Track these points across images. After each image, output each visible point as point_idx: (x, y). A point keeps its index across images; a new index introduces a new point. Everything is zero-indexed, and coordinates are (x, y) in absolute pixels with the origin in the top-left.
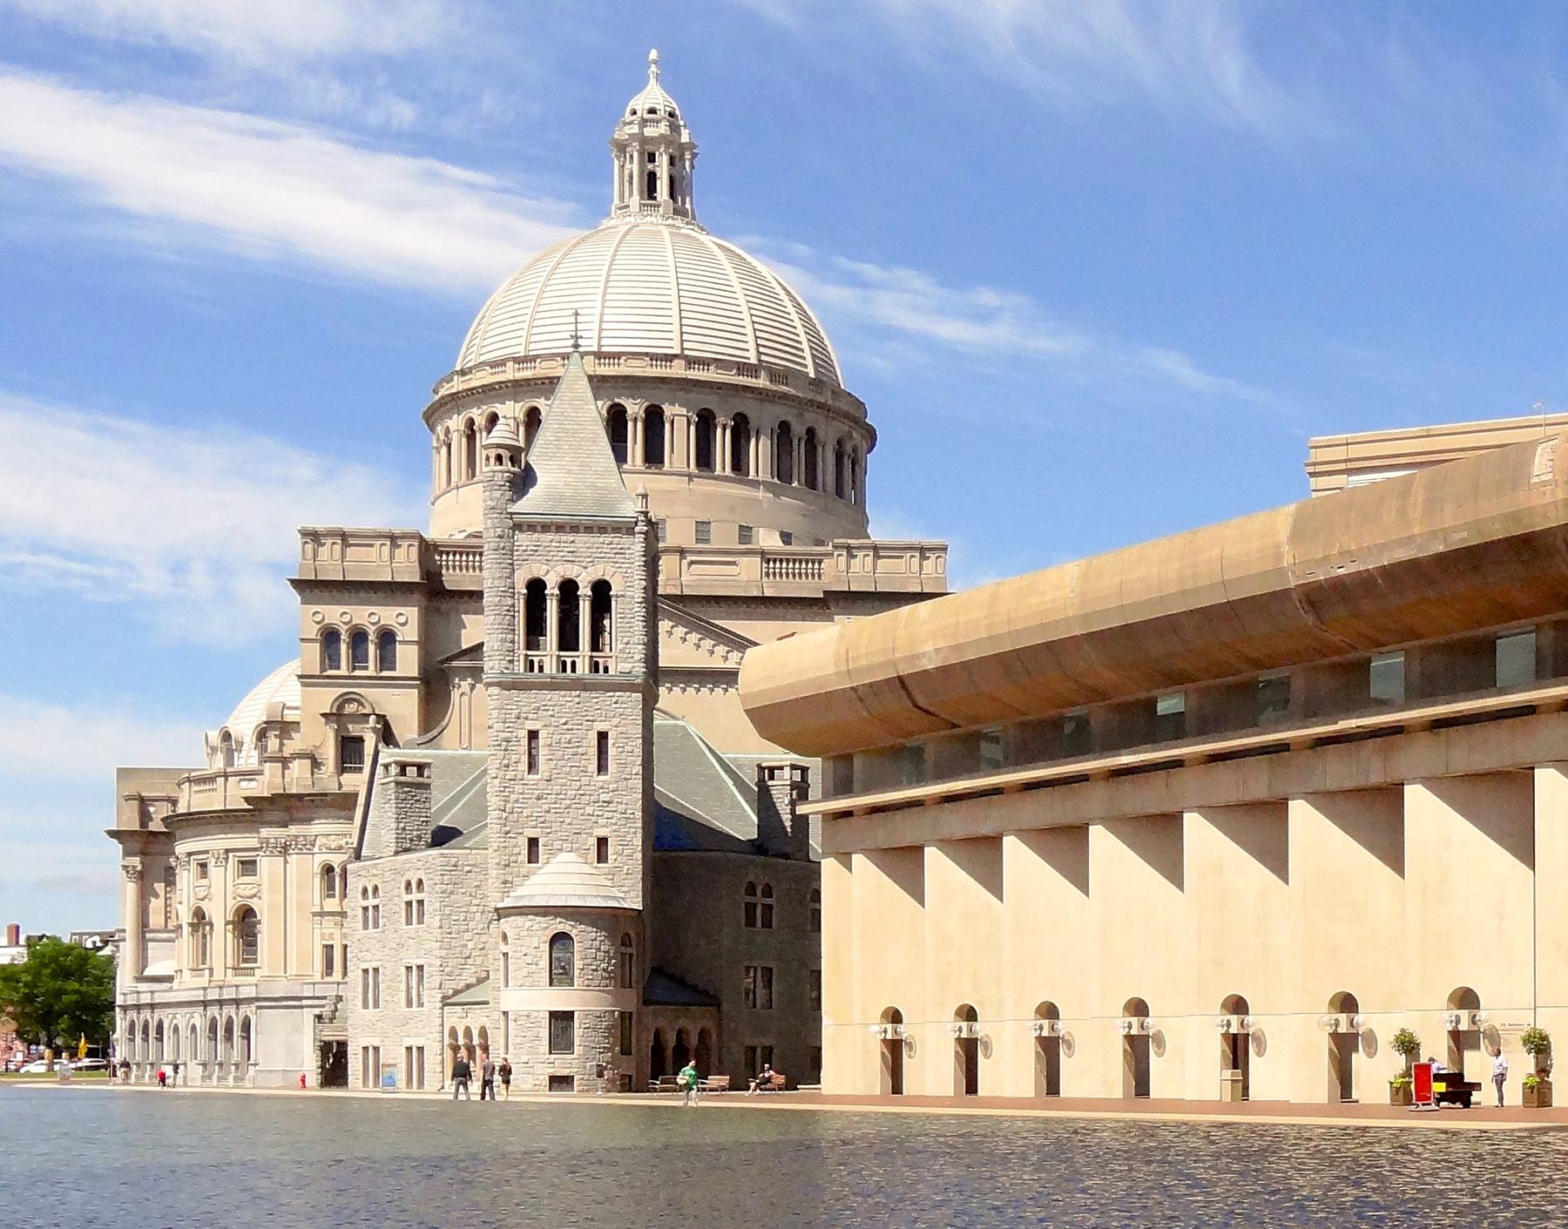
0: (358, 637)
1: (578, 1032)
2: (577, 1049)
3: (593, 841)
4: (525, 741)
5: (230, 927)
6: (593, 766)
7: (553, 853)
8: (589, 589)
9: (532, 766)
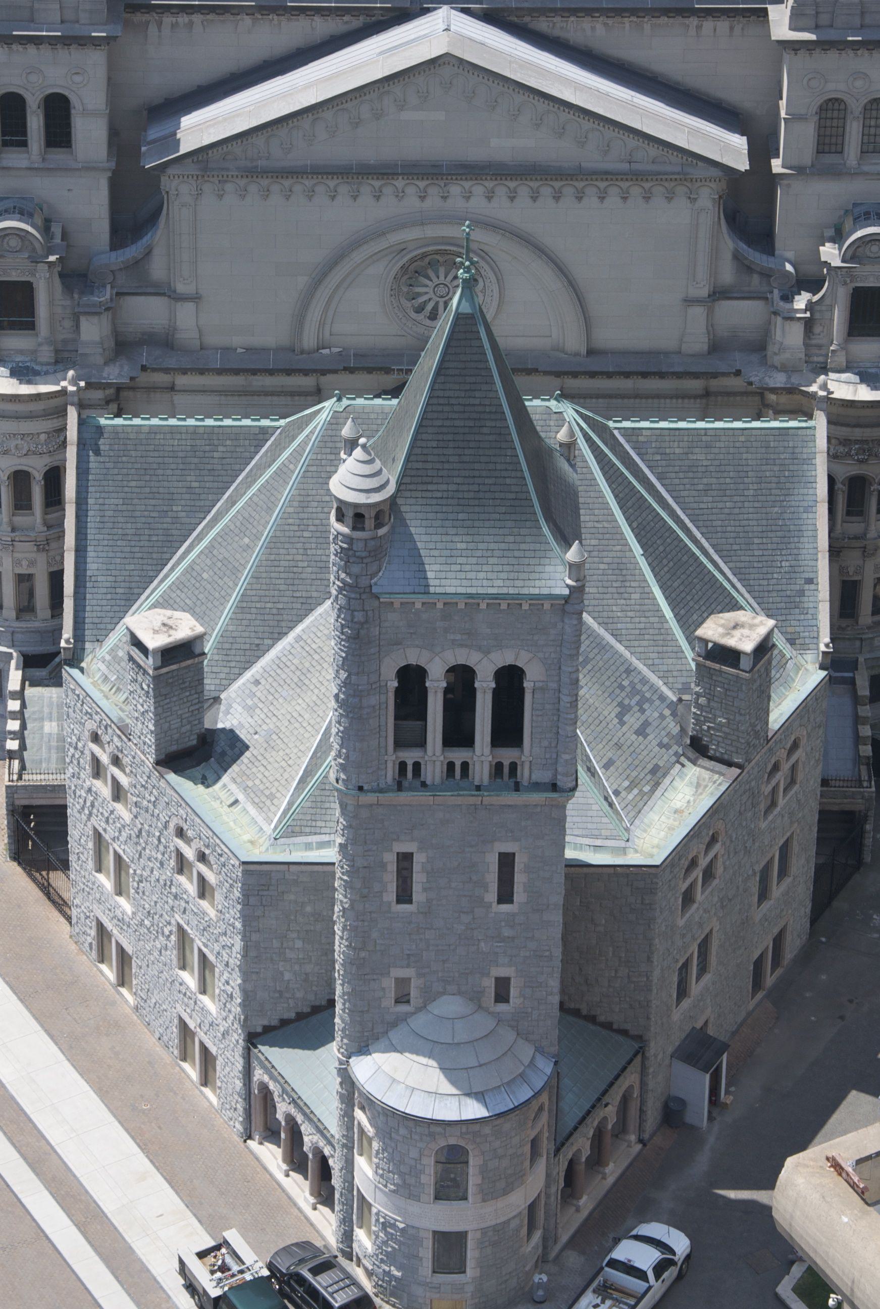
1: (472, 1254)
2: (471, 1270)
3: (489, 984)
4: (393, 867)
6: (492, 895)
7: (429, 997)
8: (491, 677)
9: (404, 896)
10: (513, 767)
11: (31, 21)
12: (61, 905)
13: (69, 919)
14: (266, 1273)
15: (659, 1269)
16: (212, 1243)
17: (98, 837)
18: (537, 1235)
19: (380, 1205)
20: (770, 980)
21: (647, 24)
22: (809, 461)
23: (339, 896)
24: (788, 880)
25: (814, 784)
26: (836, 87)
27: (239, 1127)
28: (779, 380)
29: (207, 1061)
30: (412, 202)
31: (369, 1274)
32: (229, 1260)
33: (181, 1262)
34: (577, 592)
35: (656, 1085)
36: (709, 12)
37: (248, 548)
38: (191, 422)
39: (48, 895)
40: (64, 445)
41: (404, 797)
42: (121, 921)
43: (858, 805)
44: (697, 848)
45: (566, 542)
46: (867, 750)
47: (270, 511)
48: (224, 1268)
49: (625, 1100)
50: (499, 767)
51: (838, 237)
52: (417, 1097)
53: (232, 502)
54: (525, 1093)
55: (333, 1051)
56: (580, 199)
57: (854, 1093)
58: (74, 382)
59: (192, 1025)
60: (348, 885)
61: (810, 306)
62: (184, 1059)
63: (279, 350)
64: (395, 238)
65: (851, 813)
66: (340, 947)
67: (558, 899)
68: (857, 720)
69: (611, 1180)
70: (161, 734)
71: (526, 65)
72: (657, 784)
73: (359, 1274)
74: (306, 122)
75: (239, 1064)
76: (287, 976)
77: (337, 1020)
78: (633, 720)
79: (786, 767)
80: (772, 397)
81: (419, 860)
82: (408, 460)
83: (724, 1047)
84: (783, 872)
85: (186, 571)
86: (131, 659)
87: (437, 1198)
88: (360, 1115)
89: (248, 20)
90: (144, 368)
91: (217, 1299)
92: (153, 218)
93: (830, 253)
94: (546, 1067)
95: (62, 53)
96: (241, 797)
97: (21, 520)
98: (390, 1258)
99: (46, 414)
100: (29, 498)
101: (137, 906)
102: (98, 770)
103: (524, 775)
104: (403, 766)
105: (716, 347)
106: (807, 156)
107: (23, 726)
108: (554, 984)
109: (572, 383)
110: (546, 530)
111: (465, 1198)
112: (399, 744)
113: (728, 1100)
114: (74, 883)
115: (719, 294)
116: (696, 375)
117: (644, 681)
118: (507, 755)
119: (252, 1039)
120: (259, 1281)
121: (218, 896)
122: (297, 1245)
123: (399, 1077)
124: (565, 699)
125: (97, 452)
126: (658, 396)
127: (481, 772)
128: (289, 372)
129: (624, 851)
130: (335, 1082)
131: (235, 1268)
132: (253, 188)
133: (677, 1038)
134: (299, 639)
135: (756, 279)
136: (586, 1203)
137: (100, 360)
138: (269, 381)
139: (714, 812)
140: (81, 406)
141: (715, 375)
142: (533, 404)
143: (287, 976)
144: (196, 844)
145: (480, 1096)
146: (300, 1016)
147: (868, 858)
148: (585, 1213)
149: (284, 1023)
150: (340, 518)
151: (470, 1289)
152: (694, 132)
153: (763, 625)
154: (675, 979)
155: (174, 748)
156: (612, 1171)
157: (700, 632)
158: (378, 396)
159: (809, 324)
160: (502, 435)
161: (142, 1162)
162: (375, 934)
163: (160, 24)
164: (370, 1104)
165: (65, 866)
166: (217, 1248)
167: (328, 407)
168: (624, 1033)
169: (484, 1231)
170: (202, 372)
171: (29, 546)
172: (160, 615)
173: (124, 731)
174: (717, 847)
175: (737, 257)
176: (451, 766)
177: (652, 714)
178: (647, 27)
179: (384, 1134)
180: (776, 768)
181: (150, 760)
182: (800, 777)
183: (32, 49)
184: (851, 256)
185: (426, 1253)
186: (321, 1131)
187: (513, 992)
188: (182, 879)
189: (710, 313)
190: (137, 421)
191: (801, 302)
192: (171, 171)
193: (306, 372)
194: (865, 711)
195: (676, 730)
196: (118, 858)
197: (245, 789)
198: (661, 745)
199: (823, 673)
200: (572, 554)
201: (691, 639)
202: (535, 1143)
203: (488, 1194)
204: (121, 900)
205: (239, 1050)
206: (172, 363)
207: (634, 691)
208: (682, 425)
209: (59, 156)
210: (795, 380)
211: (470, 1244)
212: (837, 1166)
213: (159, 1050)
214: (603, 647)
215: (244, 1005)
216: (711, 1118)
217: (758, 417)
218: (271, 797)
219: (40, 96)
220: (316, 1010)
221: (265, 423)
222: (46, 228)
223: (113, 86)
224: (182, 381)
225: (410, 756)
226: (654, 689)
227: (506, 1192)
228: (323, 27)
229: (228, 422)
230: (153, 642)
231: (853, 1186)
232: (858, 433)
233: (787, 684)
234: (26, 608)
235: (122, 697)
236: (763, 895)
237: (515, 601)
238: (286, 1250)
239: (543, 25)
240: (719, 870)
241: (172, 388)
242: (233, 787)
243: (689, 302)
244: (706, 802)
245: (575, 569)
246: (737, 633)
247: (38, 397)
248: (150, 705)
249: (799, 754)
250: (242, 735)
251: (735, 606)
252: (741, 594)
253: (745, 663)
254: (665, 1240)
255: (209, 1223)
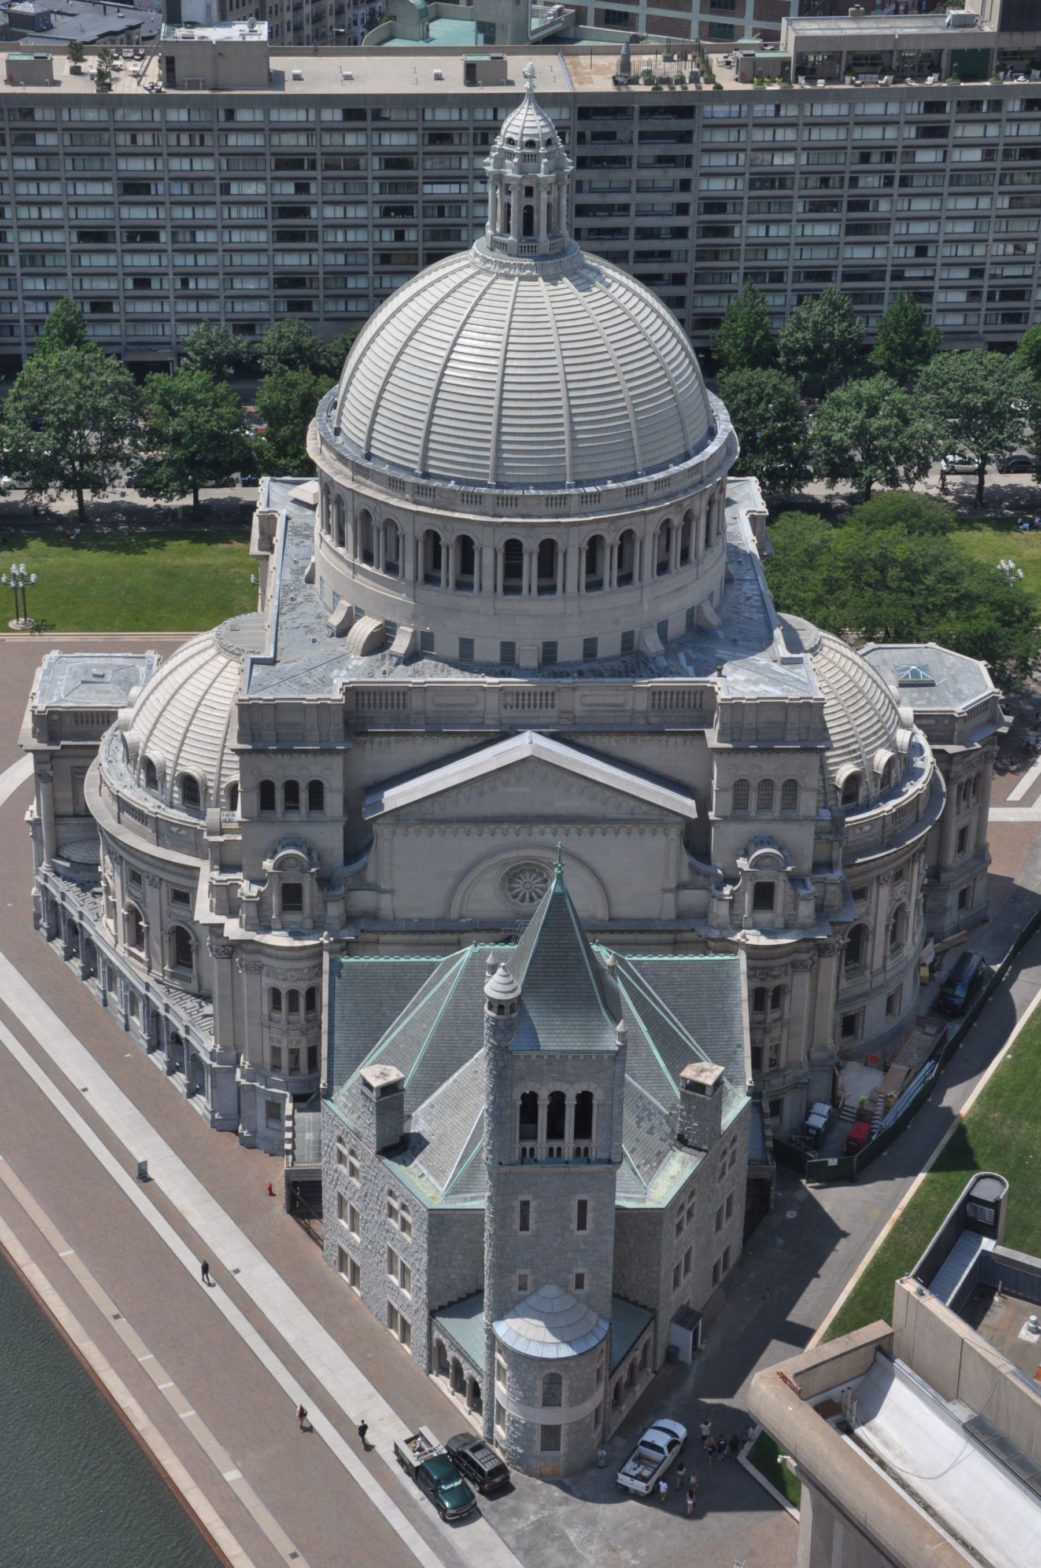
0: (291, 788)
1: (563, 1438)
2: (563, 1448)
3: (572, 1278)
4: (518, 1210)
5: (166, 938)
6: (574, 1225)
7: (538, 1285)
9: (524, 1226)
10: (586, 1150)
11: (303, 742)
12: (317, 1239)
13: (322, 1247)
14: (445, 1451)
15: (671, 1445)
16: (411, 1435)
17: (341, 1198)
18: (600, 1427)
19: (510, 1411)
20: (721, 1277)
21: (639, 740)
22: (737, 978)
23: (487, 1227)
24: (731, 1218)
25: (744, 1162)
26: (744, 773)
27: (424, 1366)
28: (716, 934)
29: (405, 1328)
30: (523, 837)
31: (504, 1452)
32: (423, 1445)
33: (396, 1446)
34: (623, 1048)
35: (662, 1338)
36: (672, 733)
37: (426, 1030)
38: (392, 960)
39: (309, 1234)
40: (319, 974)
41: (526, 1168)
42: (354, 1247)
43: (767, 1175)
44: (684, 1198)
45: (616, 1020)
46: (770, 1144)
47: (438, 1009)
48: (420, 1449)
49: (646, 1347)
50: (578, 1151)
51: (746, 854)
52: (532, 1345)
53: (416, 1004)
54: (594, 1342)
55: (482, 1318)
56: (604, 834)
57: (774, 1342)
58: (327, 938)
59: (396, 1306)
60: (493, 1220)
61: (732, 893)
62: (391, 1327)
63: (437, 920)
64: (503, 857)
65: (761, 1180)
66: (487, 1257)
67: (611, 1226)
68: (764, 1126)
69: (638, 1395)
70: (380, 1136)
71: (574, 762)
72: (660, 1162)
73: (498, 1452)
74: (453, 794)
75: (425, 1329)
76: (453, 1276)
77: (485, 1300)
78: (645, 1125)
79: (730, 1152)
80: (712, 944)
81: (533, 1205)
82: (527, 975)
83: (699, 1316)
84: (729, 1214)
85: (390, 1044)
86: (363, 1093)
87: (545, 1404)
88: (499, 1357)
89: (420, 739)
90: (363, 931)
91: (418, 1468)
92: (368, 847)
93: (743, 863)
94: (605, 1327)
95: (320, 759)
96: (425, 1172)
97: (292, 1018)
98: (517, 1442)
99: (308, 958)
100: (297, 1005)
101: (364, 1237)
102: (341, 1158)
103: (593, 1154)
104: (524, 1150)
105: (680, 917)
106: (728, 811)
107: (294, 1136)
108: (609, 1276)
109: (608, 937)
110: (604, 1014)
111: (560, 1405)
112: (522, 1138)
113: (703, 1347)
114: (326, 1226)
115: (681, 886)
116: (670, 932)
117: (650, 1103)
118: (583, 1144)
119: (433, 1314)
120: (441, 1457)
121: (413, 1230)
122: (462, 1435)
123: (522, 1333)
124: (616, 1110)
125: (340, 977)
126: (648, 944)
127: (568, 1153)
128: (443, 932)
129: (644, 1200)
130: (483, 1338)
131: (427, 1449)
132: (424, 830)
133: (673, 1311)
134: (455, 1081)
135: (701, 878)
136: (625, 1408)
137: (338, 927)
138: (432, 938)
139: (693, 1177)
140: (331, 953)
141: (680, 932)
142: (594, 947)
143: (453, 1276)
144: (401, 1199)
145: (569, 1343)
146: (461, 1300)
147: (772, 1206)
148: (625, 1414)
149: (451, 1304)
150: (490, 1008)
151: (562, 1459)
152: (666, 797)
153: (719, 1070)
154: (673, 1275)
155: (387, 1144)
156: (639, 1389)
157: (682, 1074)
158: (497, 943)
159: (732, 903)
160: (581, 960)
161: (369, 1388)
162: (508, 1249)
163: (372, 742)
164: (505, 1349)
165: (320, 1216)
166: (416, 1437)
167: (468, 951)
168: (645, 1307)
169: (571, 1425)
170: (395, 932)
171: (298, 1033)
172: (378, 1068)
173: (358, 1135)
174: (694, 1199)
175: (691, 866)
176: (551, 1150)
177: (655, 1122)
178: (639, 741)
179: (513, 1367)
180: (725, 1153)
181: (373, 1152)
182: (737, 1158)
183: (303, 756)
184: (755, 865)
185: (537, 1438)
186: (475, 1366)
187: (586, 1282)
188: (392, 1221)
189: (677, 898)
190: (362, 960)
191: (727, 890)
192: (379, 821)
193: (452, 932)
194: (768, 1121)
195: (669, 1131)
196: (353, 1210)
197: (428, 1167)
198: (661, 1139)
199: (748, 1099)
200: (620, 1027)
201: (677, 1078)
202: (599, 1371)
203: (573, 1402)
204: (354, 1235)
205: (425, 1320)
206: (378, 928)
207: (645, 1109)
208: (666, 958)
209: (316, 815)
210: (725, 933)
211: (563, 1433)
212: (784, 1378)
213: (376, 1322)
214: (630, 1084)
215: (428, 1294)
216: (693, 1358)
217: (705, 954)
218: (443, 1172)
219: (307, 782)
220: (469, 1296)
221: (433, 959)
222: (309, 854)
223: (347, 777)
224: (383, 938)
225: (528, 1145)
226: (657, 1108)
227: (583, 1400)
228: (461, 743)
229: (412, 959)
230: (376, 1083)
231: (793, 1389)
232: (760, 963)
233: (729, 1105)
234: (294, 1069)
235: (355, 1116)
236: (718, 1227)
237: (588, 1054)
238: (455, 1438)
239: (582, 740)
240: (696, 1212)
241: (377, 942)
242: (421, 1167)
243: (665, 891)
244: (688, 1172)
245: (622, 1036)
246: (704, 1074)
247: (304, 948)
248: (374, 1119)
249: (737, 1144)
250: (425, 1136)
251: (699, 1060)
252: (701, 1053)
253: (708, 1091)
254: (673, 1429)
255: (410, 1423)
